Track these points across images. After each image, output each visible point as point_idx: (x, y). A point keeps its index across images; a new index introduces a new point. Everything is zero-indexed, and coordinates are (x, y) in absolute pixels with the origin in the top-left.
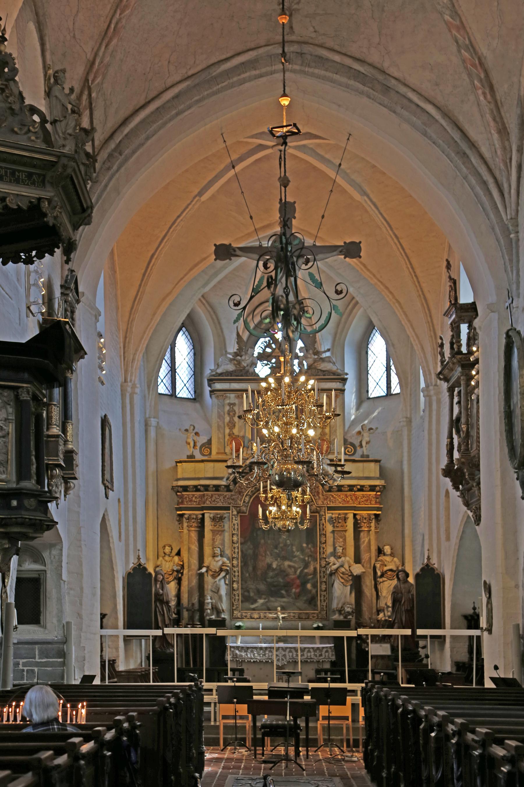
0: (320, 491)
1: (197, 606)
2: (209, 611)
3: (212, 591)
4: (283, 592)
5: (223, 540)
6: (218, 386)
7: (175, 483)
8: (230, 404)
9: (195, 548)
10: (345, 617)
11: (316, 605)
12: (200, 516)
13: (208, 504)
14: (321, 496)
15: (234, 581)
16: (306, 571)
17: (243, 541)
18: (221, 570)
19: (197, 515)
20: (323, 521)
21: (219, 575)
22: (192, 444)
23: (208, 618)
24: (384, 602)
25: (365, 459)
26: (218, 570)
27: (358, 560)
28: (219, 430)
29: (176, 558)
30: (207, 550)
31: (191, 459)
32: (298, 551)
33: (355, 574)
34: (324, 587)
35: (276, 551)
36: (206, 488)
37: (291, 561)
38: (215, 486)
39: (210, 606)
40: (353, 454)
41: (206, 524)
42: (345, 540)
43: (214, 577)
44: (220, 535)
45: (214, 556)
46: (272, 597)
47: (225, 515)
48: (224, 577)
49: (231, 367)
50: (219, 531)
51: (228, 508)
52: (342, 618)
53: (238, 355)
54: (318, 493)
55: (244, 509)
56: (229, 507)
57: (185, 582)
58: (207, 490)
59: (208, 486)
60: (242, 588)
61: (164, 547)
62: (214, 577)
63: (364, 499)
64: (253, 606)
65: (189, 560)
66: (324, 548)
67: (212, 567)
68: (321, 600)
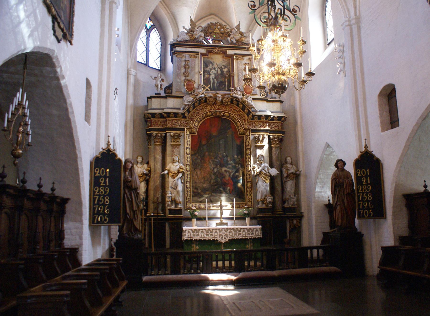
0: (246, 119)
1: (160, 200)
2: (169, 203)
3: (172, 187)
4: (221, 189)
5: (179, 152)
6: (178, 49)
7: (146, 112)
8: (185, 61)
9: (159, 157)
11: (244, 199)
12: (164, 135)
13: (169, 126)
14: (246, 122)
15: (187, 182)
16: (237, 174)
17: (193, 153)
18: (179, 172)
19: (161, 134)
20: (249, 140)
21: (177, 175)
22: (159, 86)
23: (169, 208)
24: (288, 195)
26: (176, 172)
27: (271, 166)
29: (146, 166)
30: (168, 159)
31: (158, 96)
32: (231, 160)
33: (273, 175)
34: (249, 185)
35: (216, 160)
36: (168, 114)
37: (226, 167)
38: (174, 113)
40: (266, 97)
41: (167, 140)
43: (173, 177)
44: (178, 148)
45: (173, 162)
46: (213, 193)
47: (182, 134)
48: (181, 178)
49: (187, 38)
50: (177, 145)
51: (183, 130)
52: (264, 206)
53: (192, 31)
54: (245, 120)
55: (195, 130)
56: (184, 129)
57: (151, 184)
58: (169, 117)
59: (170, 113)
60: (192, 187)
61: (137, 157)
62: (173, 177)
63: (274, 126)
64: (200, 200)
65: (154, 166)
66: (249, 158)
67: (172, 170)
68: (247, 195)
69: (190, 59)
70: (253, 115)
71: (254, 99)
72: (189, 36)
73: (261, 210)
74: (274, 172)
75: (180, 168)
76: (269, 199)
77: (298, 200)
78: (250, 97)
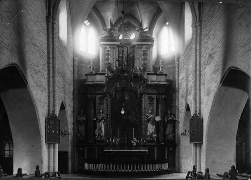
10: (152, 139)
12: (94, 97)
18: (102, 119)
25: (161, 74)
28: (102, 61)
30: (97, 111)
32: (133, 112)
34: (144, 127)
39: (97, 134)
42: (153, 106)
69: (110, 49)
70: (146, 84)
71: (148, 74)
72: (109, 33)
73: (149, 141)
74: (158, 119)
75: (103, 117)
76: (154, 135)
77: (174, 136)
78: (145, 72)
